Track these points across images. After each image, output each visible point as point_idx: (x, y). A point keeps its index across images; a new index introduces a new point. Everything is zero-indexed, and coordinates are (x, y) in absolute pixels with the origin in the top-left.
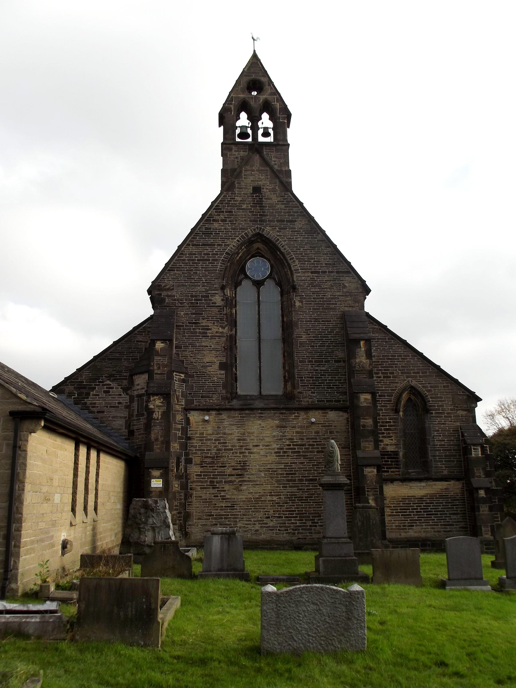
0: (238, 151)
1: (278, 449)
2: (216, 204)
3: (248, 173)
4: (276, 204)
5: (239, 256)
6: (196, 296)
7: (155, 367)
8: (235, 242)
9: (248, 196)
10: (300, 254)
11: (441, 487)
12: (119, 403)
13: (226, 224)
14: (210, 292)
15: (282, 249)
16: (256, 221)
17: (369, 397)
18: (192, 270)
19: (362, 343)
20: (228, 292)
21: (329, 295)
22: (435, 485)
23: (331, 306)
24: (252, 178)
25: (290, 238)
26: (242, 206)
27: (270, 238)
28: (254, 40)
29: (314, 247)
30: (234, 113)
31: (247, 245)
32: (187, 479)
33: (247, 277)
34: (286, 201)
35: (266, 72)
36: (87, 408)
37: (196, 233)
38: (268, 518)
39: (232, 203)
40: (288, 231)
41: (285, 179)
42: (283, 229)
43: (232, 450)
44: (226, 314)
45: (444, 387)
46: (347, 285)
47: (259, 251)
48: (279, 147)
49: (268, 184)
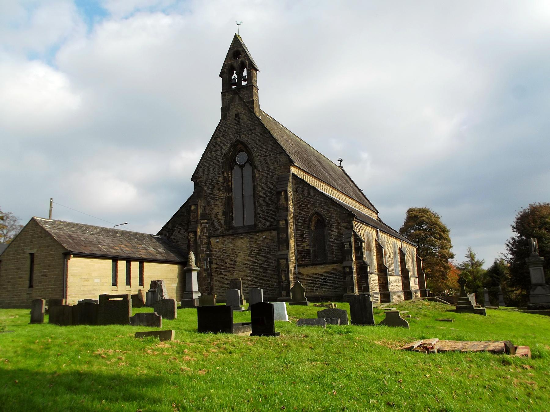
1: (249, 253)
3: (233, 106)
4: (247, 121)
6: (211, 179)
7: (192, 219)
11: (332, 267)
12: (184, 237)
14: (217, 176)
16: (237, 133)
17: (284, 222)
18: (209, 166)
19: (283, 193)
20: (226, 174)
21: (272, 167)
22: (330, 266)
23: (274, 173)
24: (235, 109)
29: (265, 142)
32: (211, 271)
33: (236, 164)
36: (172, 241)
38: (246, 288)
42: (249, 135)
43: (229, 255)
44: (225, 186)
45: (335, 210)
46: (281, 160)
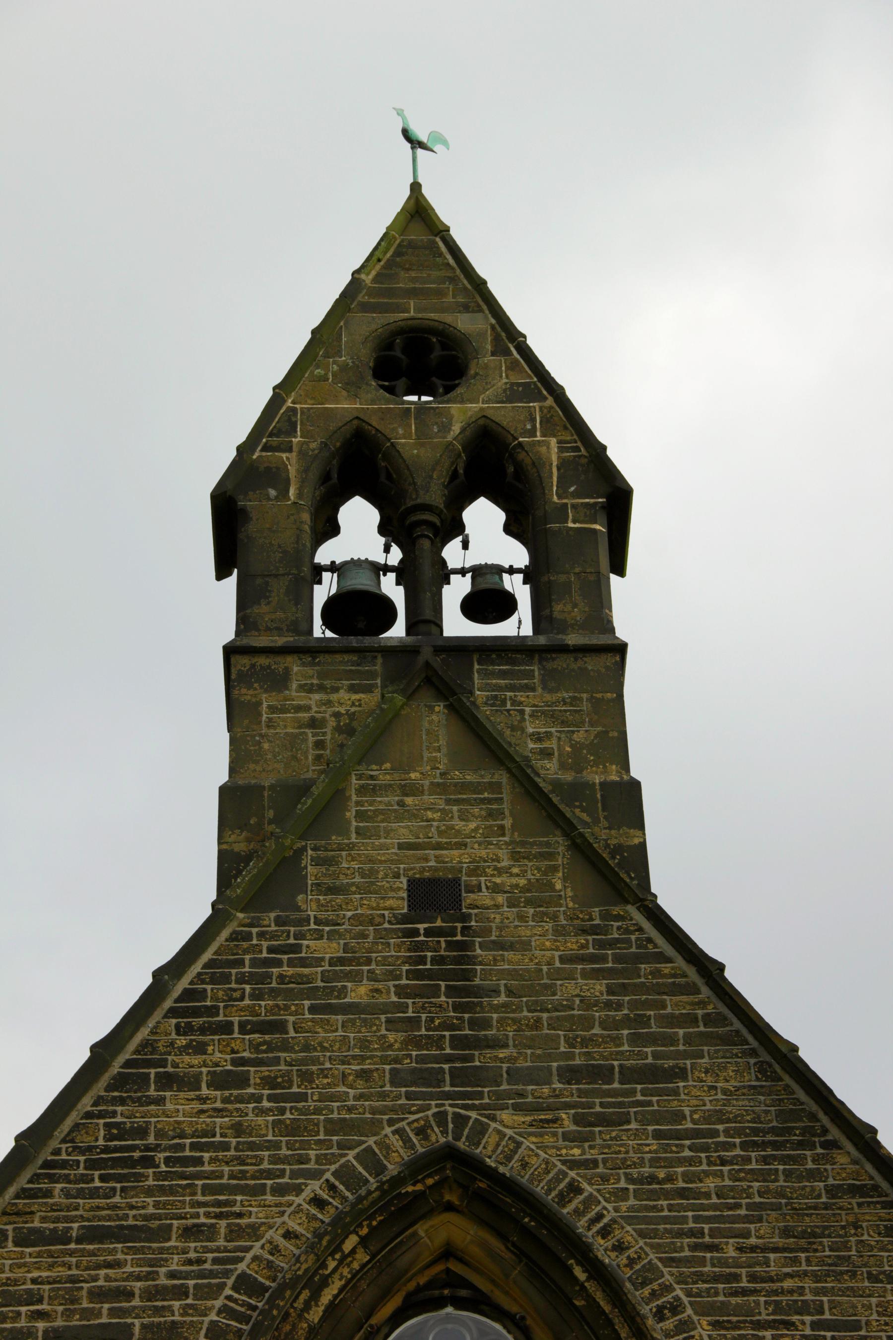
0: (321, 688)
2: (184, 983)
5: (327, 1297)
8: (299, 1209)
9: (381, 935)
10: (717, 1278)
13: (240, 1100)
15: (601, 1248)
16: (434, 1078)
24: (404, 831)
25: (652, 1179)
26: (343, 992)
27: (524, 1181)
28: (415, 143)
30: (300, 495)
31: (372, 1230)
34: (617, 959)
35: (480, 285)
37: (47, 1165)
39: (281, 978)
40: (636, 1134)
41: (603, 834)
42: (603, 1120)
47: (455, 1267)
48: (561, 662)
49: (505, 864)
